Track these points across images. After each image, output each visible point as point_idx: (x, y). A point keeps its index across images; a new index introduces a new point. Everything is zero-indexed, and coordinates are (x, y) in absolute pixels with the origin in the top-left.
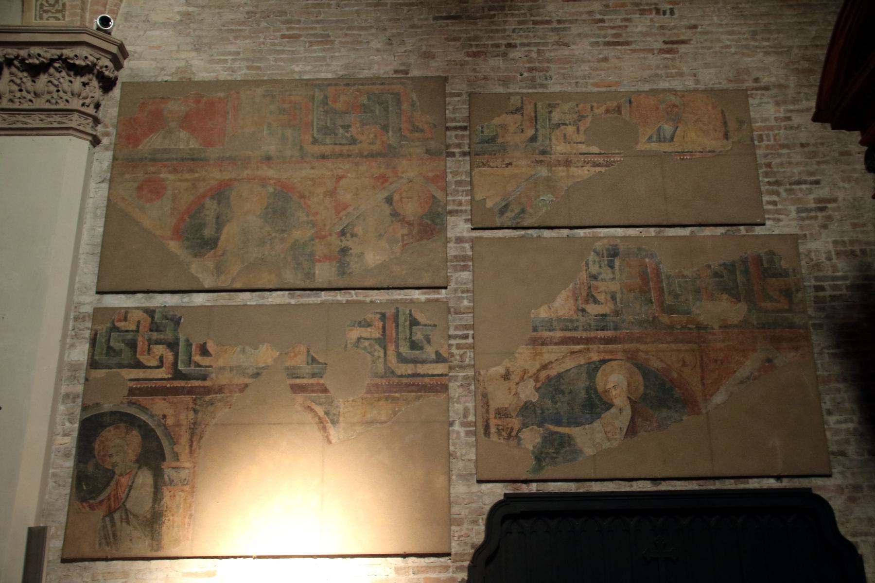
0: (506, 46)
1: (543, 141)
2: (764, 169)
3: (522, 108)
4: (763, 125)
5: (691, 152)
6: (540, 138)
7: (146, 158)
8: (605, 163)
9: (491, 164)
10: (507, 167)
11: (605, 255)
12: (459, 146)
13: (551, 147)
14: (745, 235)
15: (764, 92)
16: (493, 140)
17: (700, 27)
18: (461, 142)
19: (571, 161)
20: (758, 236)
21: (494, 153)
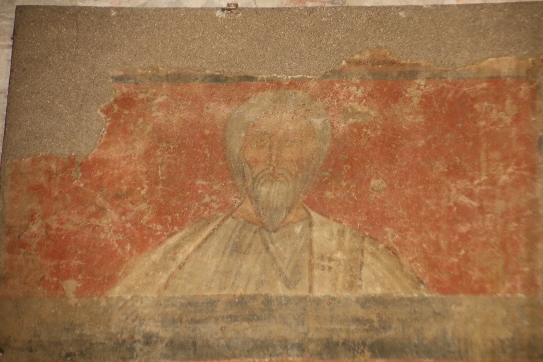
7: (149, 340)
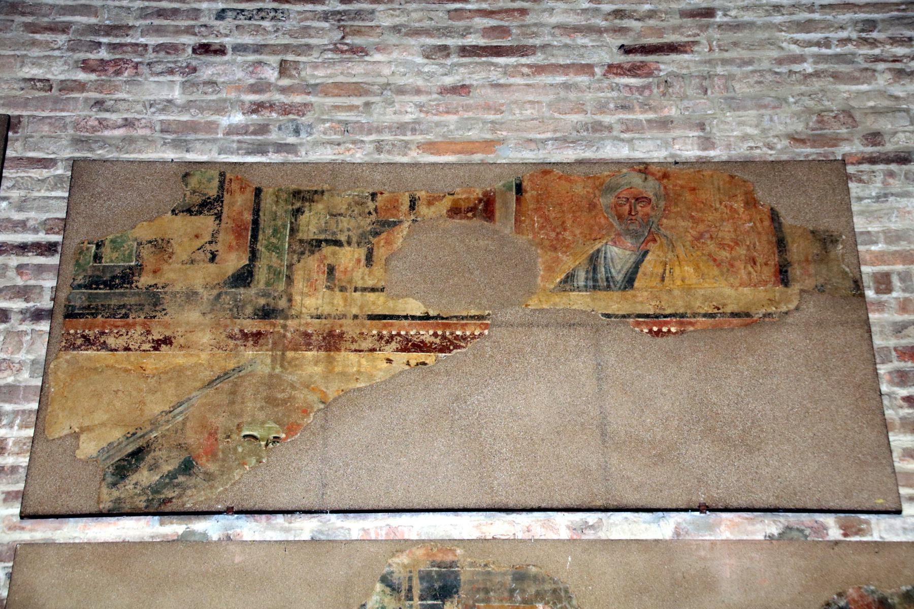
0: (194, 51)
1: (268, 284)
2: (897, 364)
3: (219, 199)
4: (893, 248)
5: (683, 316)
6: (261, 275)
8: (438, 341)
9: (111, 341)
10: (156, 349)
11: (416, 592)
12: (24, 293)
13: (290, 300)
14: (837, 543)
15: (893, 167)
16: (127, 277)
17: (720, 13)
18: (32, 282)
19: (341, 336)
20: (880, 546)
21: (123, 311)
